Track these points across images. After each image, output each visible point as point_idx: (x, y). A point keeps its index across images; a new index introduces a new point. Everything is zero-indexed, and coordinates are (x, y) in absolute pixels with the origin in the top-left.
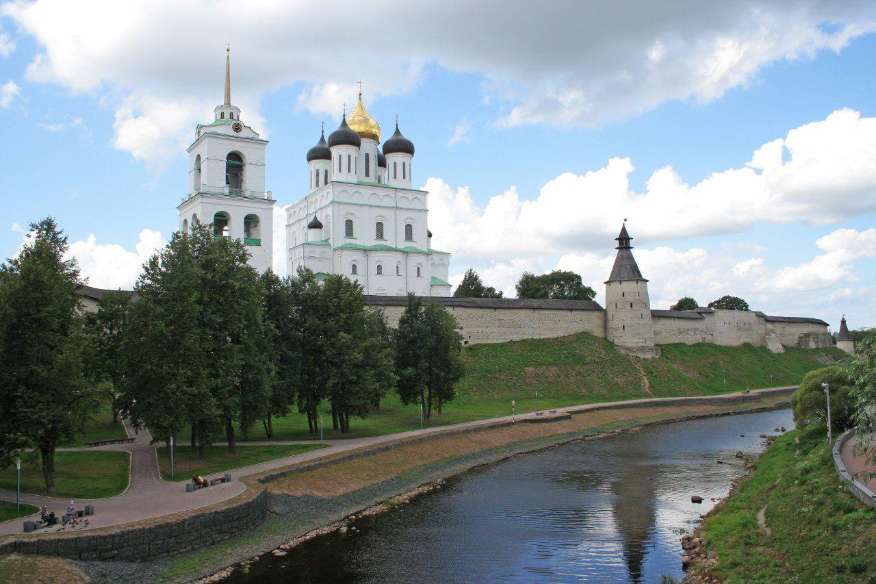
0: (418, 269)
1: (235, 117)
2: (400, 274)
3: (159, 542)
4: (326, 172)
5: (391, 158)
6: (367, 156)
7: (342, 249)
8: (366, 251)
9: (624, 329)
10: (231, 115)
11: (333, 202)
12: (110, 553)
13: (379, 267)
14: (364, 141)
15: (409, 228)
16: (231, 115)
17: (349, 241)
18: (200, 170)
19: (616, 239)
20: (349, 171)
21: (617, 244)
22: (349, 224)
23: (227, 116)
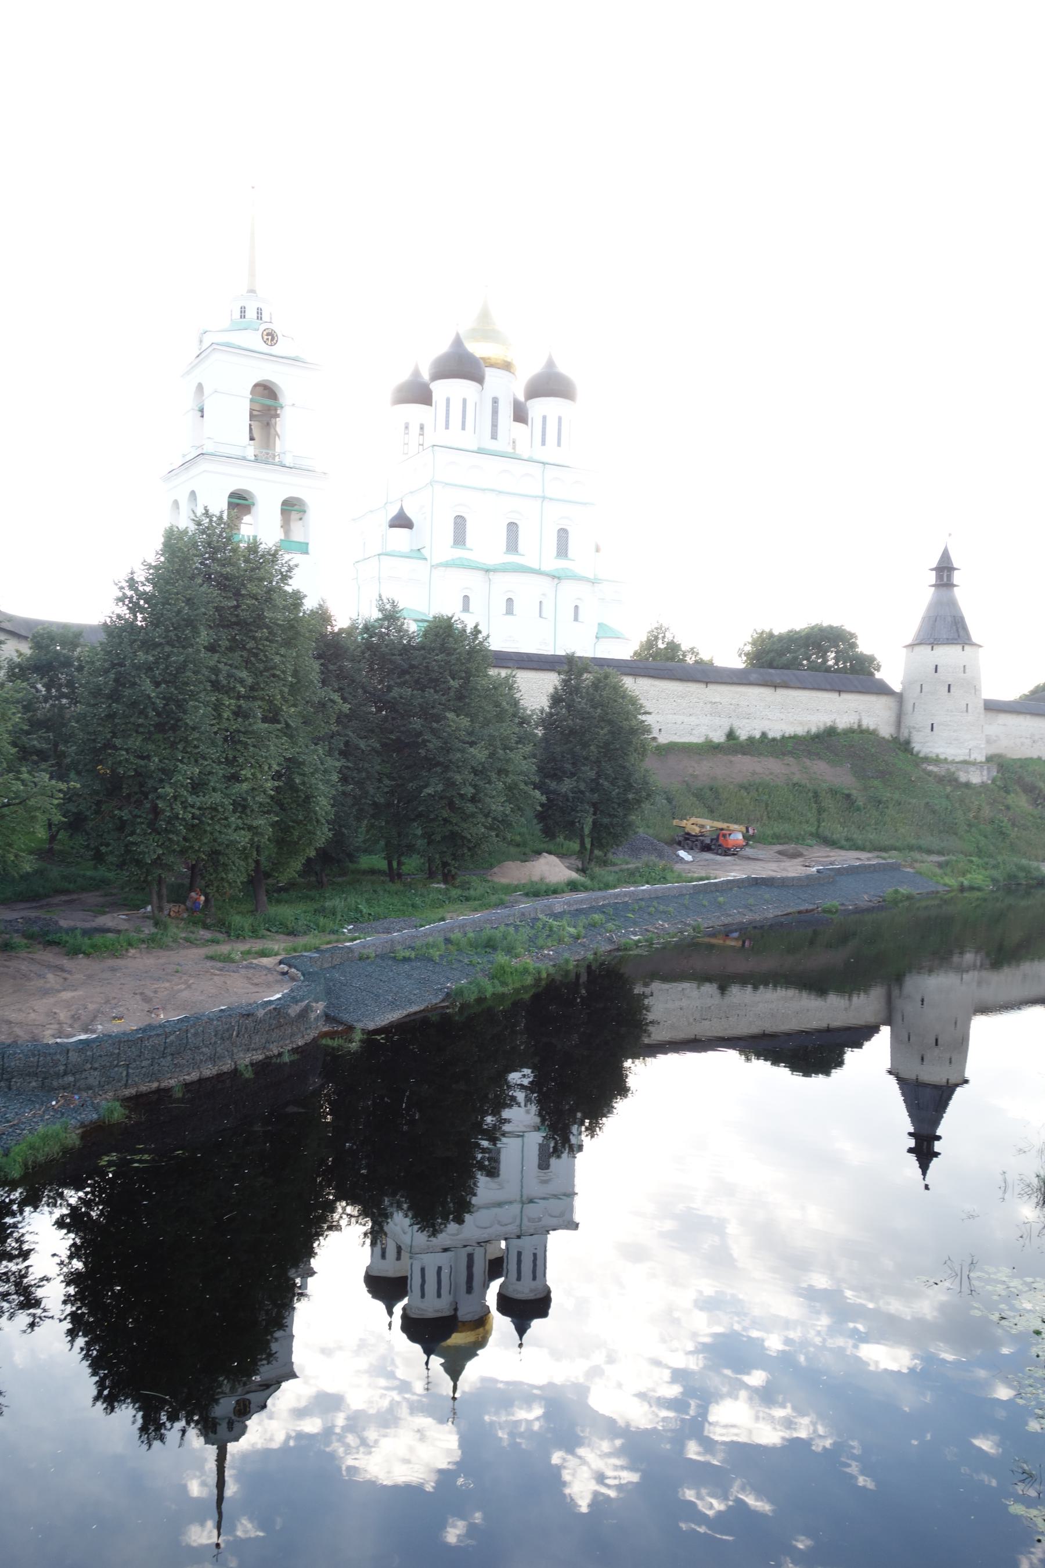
0: (576, 607)
1: (266, 317)
2: (544, 615)
3: (145, 1063)
5: (538, 408)
6: (495, 401)
7: (447, 565)
9: (932, 730)
10: (259, 313)
11: (431, 483)
12: (60, 1081)
13: (510, 601)
14: (491, 375)
15: (563, 535)
16: (259, 313)
17: (458, 553)
18: (202, 411)
19: (932, 570)
20: (463, 428)
21: (932, 577)
22: (460, 523)
23: (251, 314)
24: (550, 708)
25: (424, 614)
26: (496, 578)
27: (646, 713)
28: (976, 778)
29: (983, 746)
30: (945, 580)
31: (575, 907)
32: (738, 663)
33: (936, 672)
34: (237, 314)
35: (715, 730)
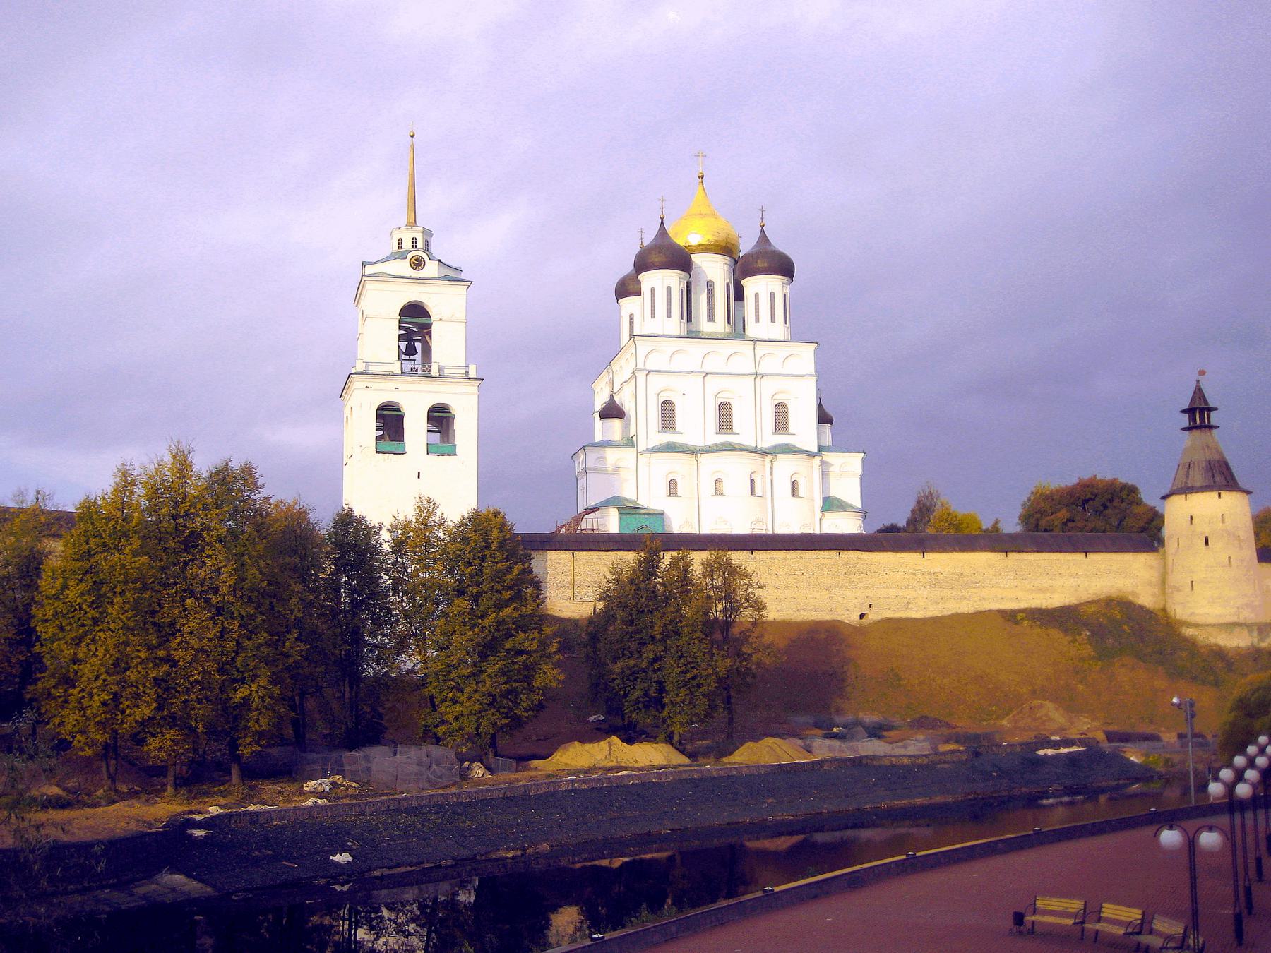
1: (420, 245)
8: (693, 451)
19: (1184, 411)
23: (407, 244)
25: (630, 501)
26: (703, 458)
29: (1256, 603)
35: (937, 603)
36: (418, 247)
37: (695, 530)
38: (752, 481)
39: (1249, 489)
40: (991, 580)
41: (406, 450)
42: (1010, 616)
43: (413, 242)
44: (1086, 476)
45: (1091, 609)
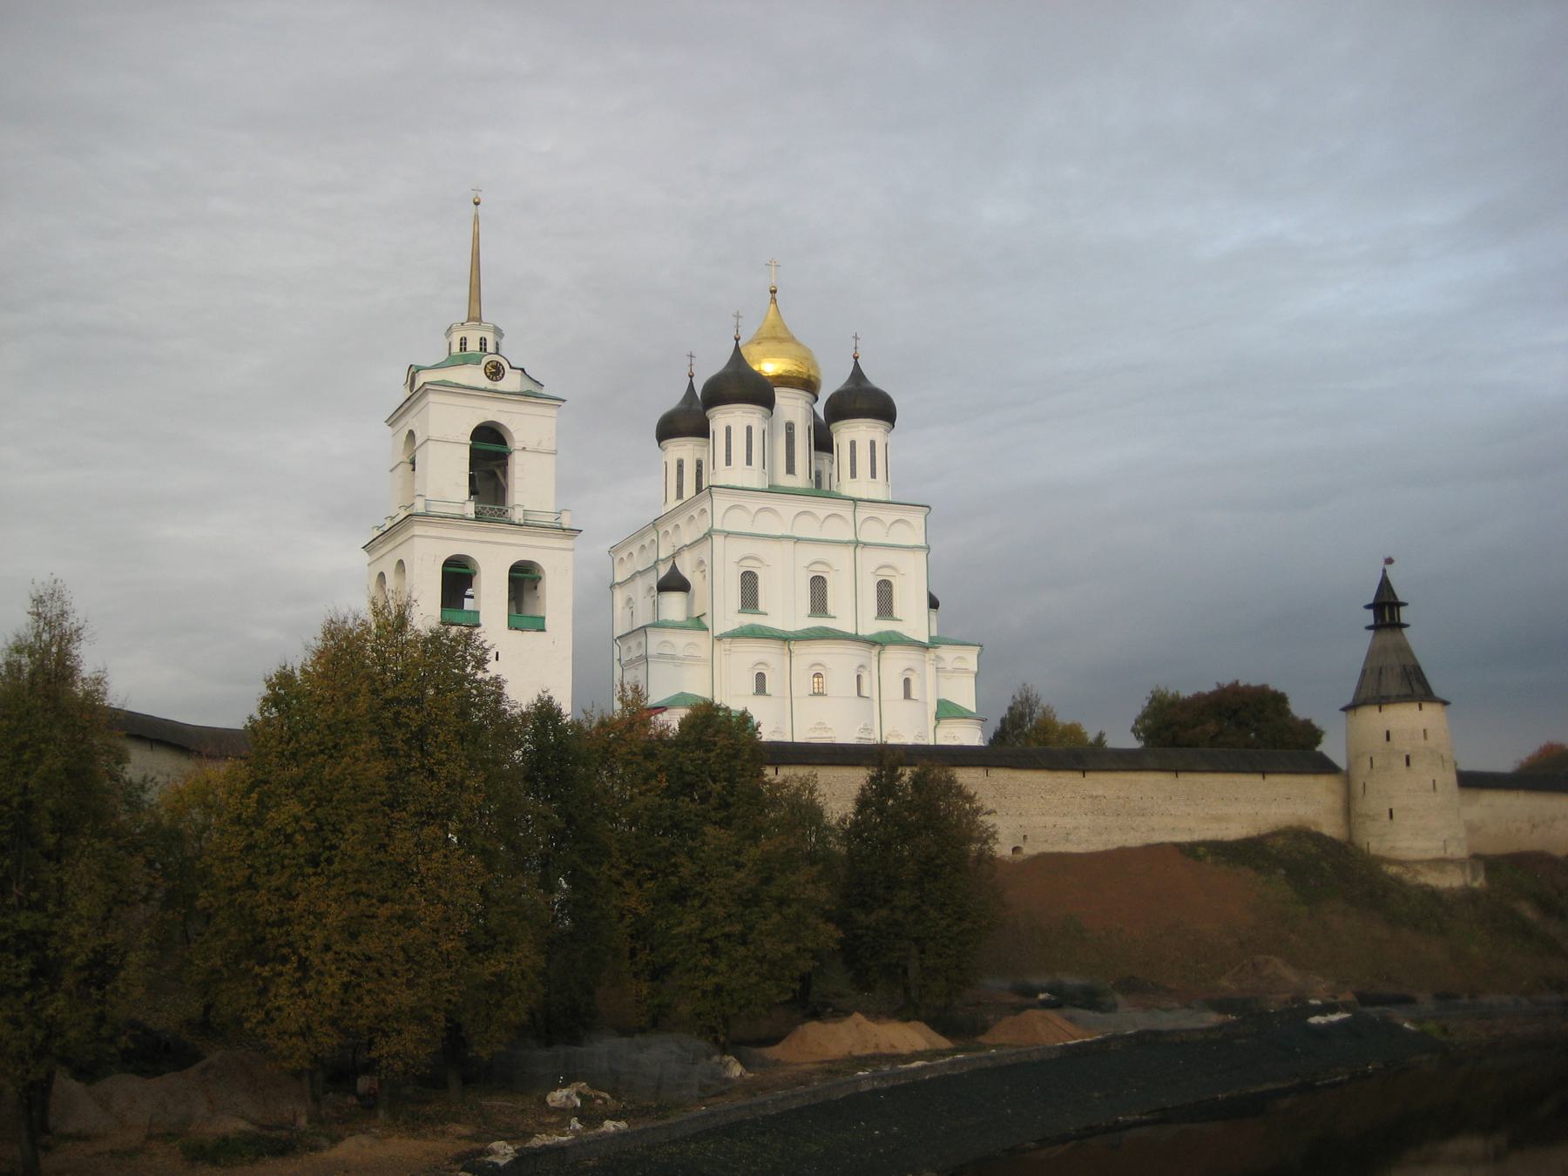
0: (907, 682)
1: (490, 348)
4: (699, 464)
8: (785, 638)
11: (708, 535)
16: (483, 342)
17: (749, 619)
18: (413, 463)
19: (1368, 607)
22: (749, 583)
23: (473, 346)
24: (856, 814)
26: (797, 648)
27: (989, 813)
28: (1451, 880)
30: (1387, 619)
31: (891, 1083)
32: (1132, 743)
33: (1388, 738)
34: (456, 349)
35: (1100, 834)
36: (488, 351)
37: (787, 738)
38: (859, 677)
39: (1447, 699)
40: (1160, 806)
41: (481, 621)
42: (1189, 851)
43: (481, 344)
44: (1227, 681)
45: (1280, 841)
